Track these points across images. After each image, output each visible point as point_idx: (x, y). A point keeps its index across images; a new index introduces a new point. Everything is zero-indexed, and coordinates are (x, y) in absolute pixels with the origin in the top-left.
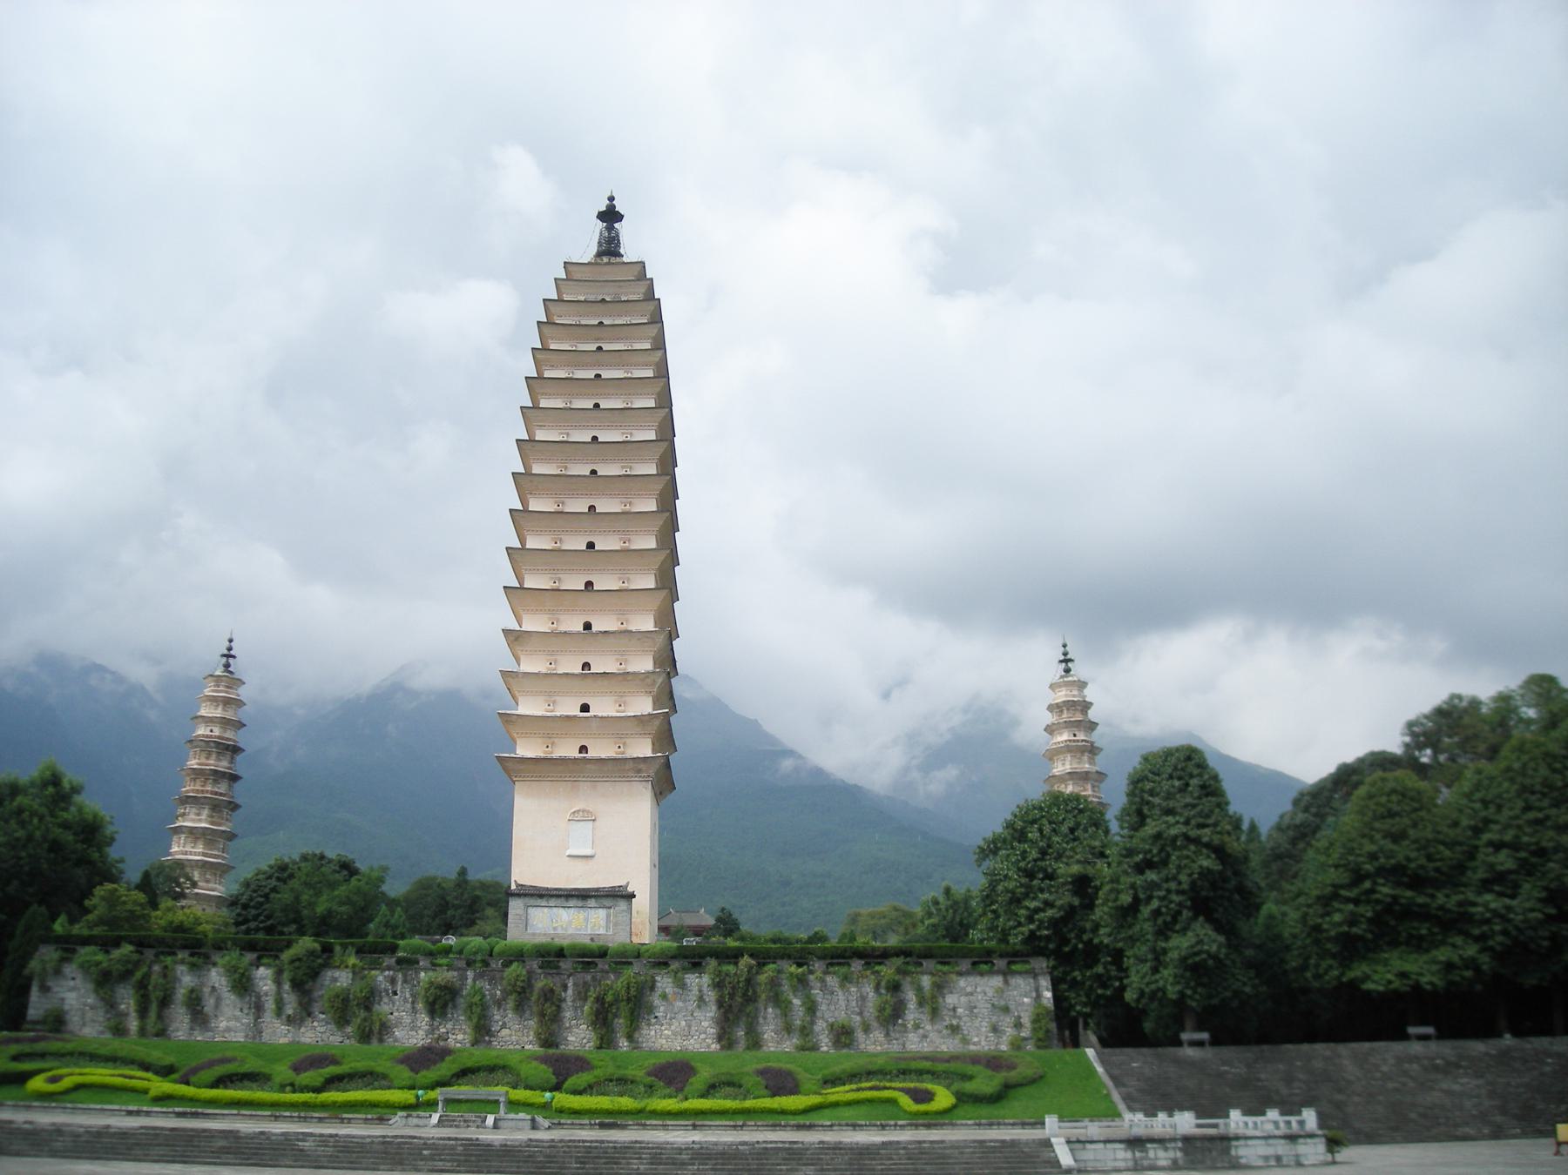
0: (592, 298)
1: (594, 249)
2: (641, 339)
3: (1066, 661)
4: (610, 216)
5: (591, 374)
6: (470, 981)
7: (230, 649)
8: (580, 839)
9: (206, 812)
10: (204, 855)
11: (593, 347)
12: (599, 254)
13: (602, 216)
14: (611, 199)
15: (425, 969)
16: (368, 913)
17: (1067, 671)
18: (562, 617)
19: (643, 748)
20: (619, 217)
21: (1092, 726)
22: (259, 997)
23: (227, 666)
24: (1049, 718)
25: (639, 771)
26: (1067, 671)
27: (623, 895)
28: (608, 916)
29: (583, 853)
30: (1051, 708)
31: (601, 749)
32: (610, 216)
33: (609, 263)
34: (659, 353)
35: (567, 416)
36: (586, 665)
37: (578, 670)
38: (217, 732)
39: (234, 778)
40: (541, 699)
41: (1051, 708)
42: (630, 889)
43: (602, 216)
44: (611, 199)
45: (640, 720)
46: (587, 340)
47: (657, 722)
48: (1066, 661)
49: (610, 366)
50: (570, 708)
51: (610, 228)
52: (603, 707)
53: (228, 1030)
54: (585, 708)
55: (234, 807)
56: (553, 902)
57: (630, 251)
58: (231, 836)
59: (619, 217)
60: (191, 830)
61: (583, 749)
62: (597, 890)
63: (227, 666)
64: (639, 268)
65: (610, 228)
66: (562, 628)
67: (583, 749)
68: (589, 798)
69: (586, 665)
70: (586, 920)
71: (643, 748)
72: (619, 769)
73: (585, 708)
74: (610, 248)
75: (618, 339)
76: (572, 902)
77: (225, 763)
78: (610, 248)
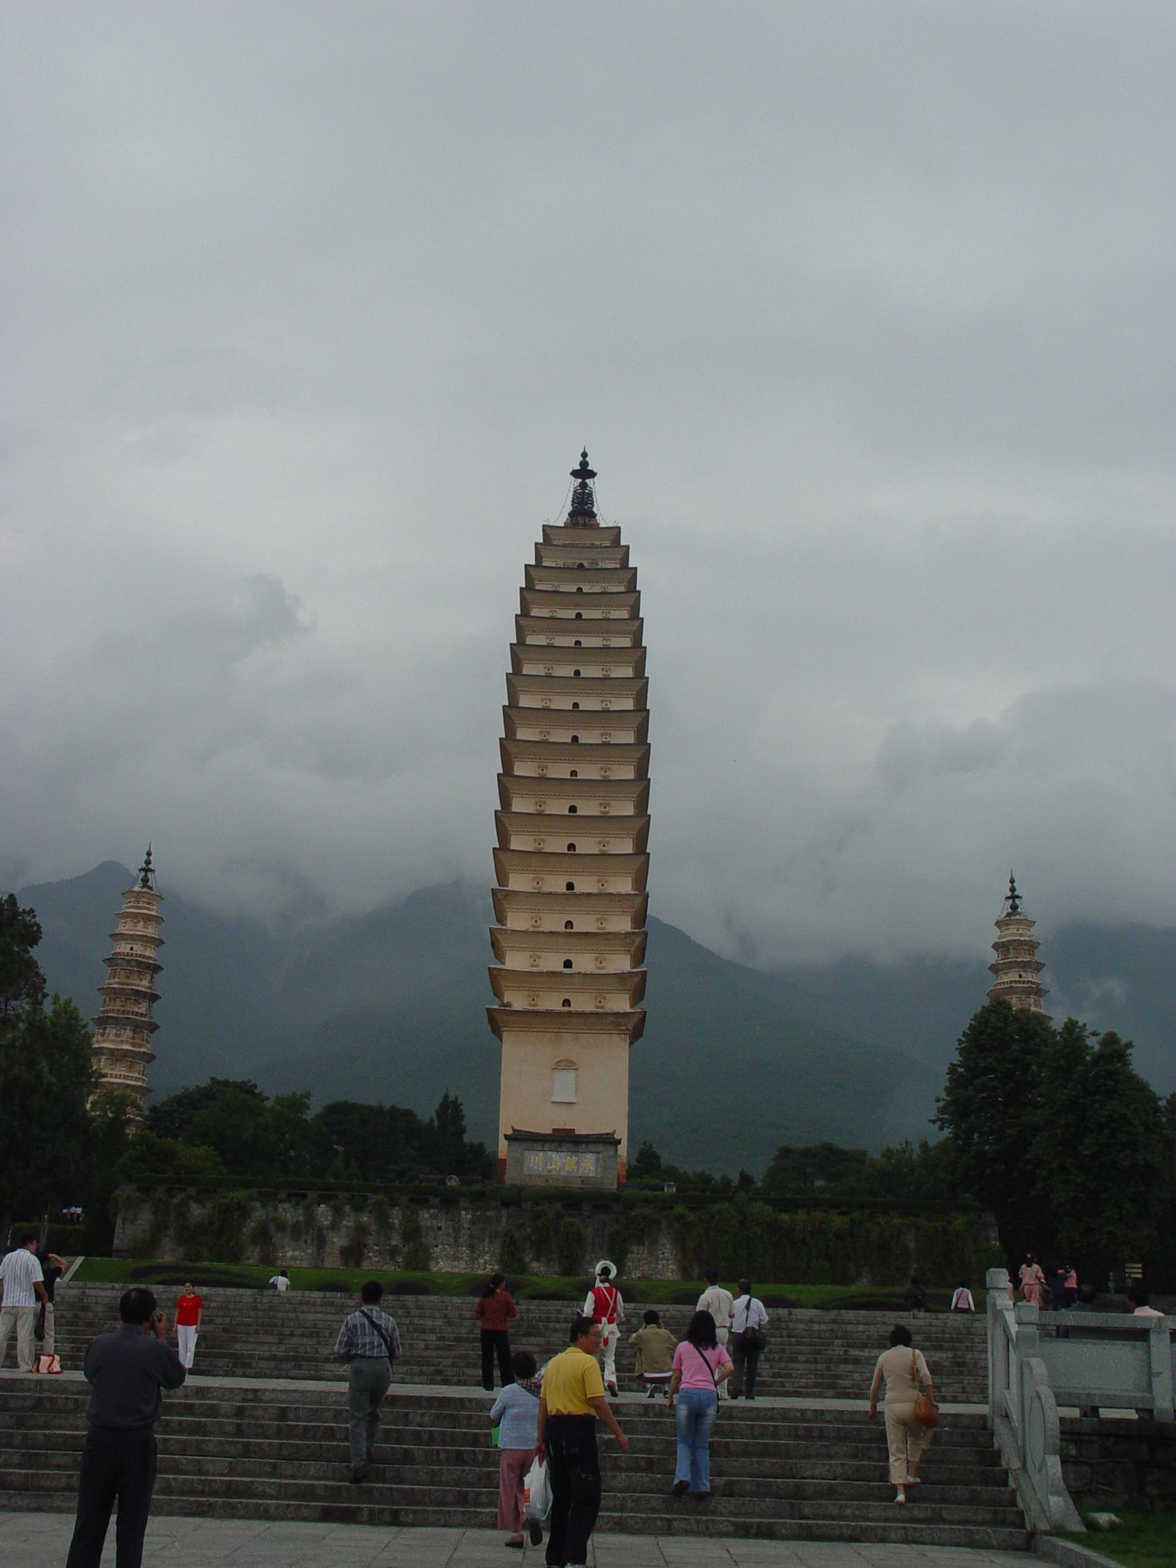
0: (570, 562)
1: (569, 508)
2: (619, 606)
3: (1013, 897)
4: (584, 473)
5: (569, 641)
6: (504, 1219)
7: (148, 862)
8: (564, 1086)
9: (129, 1033)
10: (125, 1077)
11: (571, 614)
12: (570, 515)
13: (575, 474)
14: (584, 455)
15: (465, 1209)
16: (406, 1155)
17: (1014, 907)
18: (546, 877)
19: (621, 1003)
20: (592, 474)
21: (1038, 967)
22: (320, 1230)
23: (145, 880)
24: (993, 957)
25: (619, 1025)
26: (1014, 907)
27: (609, 1141)
28: (597, 1160)
29: (563, 1097)
30: (996, 946)
31: (583, 1003)
32: (584, 473)
33: (584, 525)
34: (638, 623)
36: (569, 924)
37: (562, 929)
38: (138, 949)
39: (154, 998)
40: (528, 954)
41: (996, 946)
42: (617, 1136)
43: (575, 474)
44: (584, 455)
45: (621, 977)
46: (566, 606)
47: (636, 980)
48: (1013, 897)
49: (588, 632)
50: (552, 962)
51: (583, 485)
52: (584, 963)
53: (294, 1258)
54: (568, 964)
55: (153, 1027)
56: (547, 1146)
57: (606, 514)
58: (149, 1058)
59: (592, 474)
60: (112, 1052)
61: (567, 1002)
62: (588, 1136)
63: (145, 880)
64: (615, 532)
65: (583, 485)
66: (545, 890)
67: (567, 1002)
68: (569, 1046)
69: (569, 924)
70: (578, 1163)
71: (621, 1003)
72: (599, 1020)
73: (568, 964)
75: (596, 606)
76: (566, 1146)
77: (145, 983)
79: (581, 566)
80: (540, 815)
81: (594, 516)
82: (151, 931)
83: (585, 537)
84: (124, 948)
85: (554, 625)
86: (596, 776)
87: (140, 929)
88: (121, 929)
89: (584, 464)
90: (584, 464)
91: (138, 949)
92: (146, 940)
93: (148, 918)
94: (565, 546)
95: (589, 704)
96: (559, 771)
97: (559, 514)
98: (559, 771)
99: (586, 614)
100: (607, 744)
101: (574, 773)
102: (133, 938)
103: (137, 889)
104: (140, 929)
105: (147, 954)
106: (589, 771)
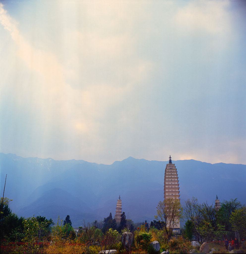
4: (170, 158)
5: (170, 177)
13: (169, 158)
17: (217, 199)
23: (120, 199)
26: (217, 199)
27: (179, 229)
32: (170, 158)
35: (169, 181)
38: (120, 207)
43: (169, 158)
48: (217, 197)
51: (170, 159)
63: (120, 199)
65: (170, 159)
74: (170, 161)
78: (170, 161)
79: (171, 168)
80: (169, 195)
81: (171, 162)
82: (121, 205)
83: (171, 165)
84: (118, 207)
85: (169, 175)
86: (174, 191)
87: (120, 205)
88: (117, 205)
89: (170, 157)
90: (170, 157)
91: (120, 207)
92: (120, 206)
93: (120, 203)
94: (169, 166)
95: (173, 183)
96: (170, 190)
97: (168, 163)
98: (170, 190)
99: (172, 174)
100: (175, 188)
101: (172, 190)
102: (119, 206)
103: (119, 200)
104: (120, 205)
105: (121, 207)
106: (174, 190)
